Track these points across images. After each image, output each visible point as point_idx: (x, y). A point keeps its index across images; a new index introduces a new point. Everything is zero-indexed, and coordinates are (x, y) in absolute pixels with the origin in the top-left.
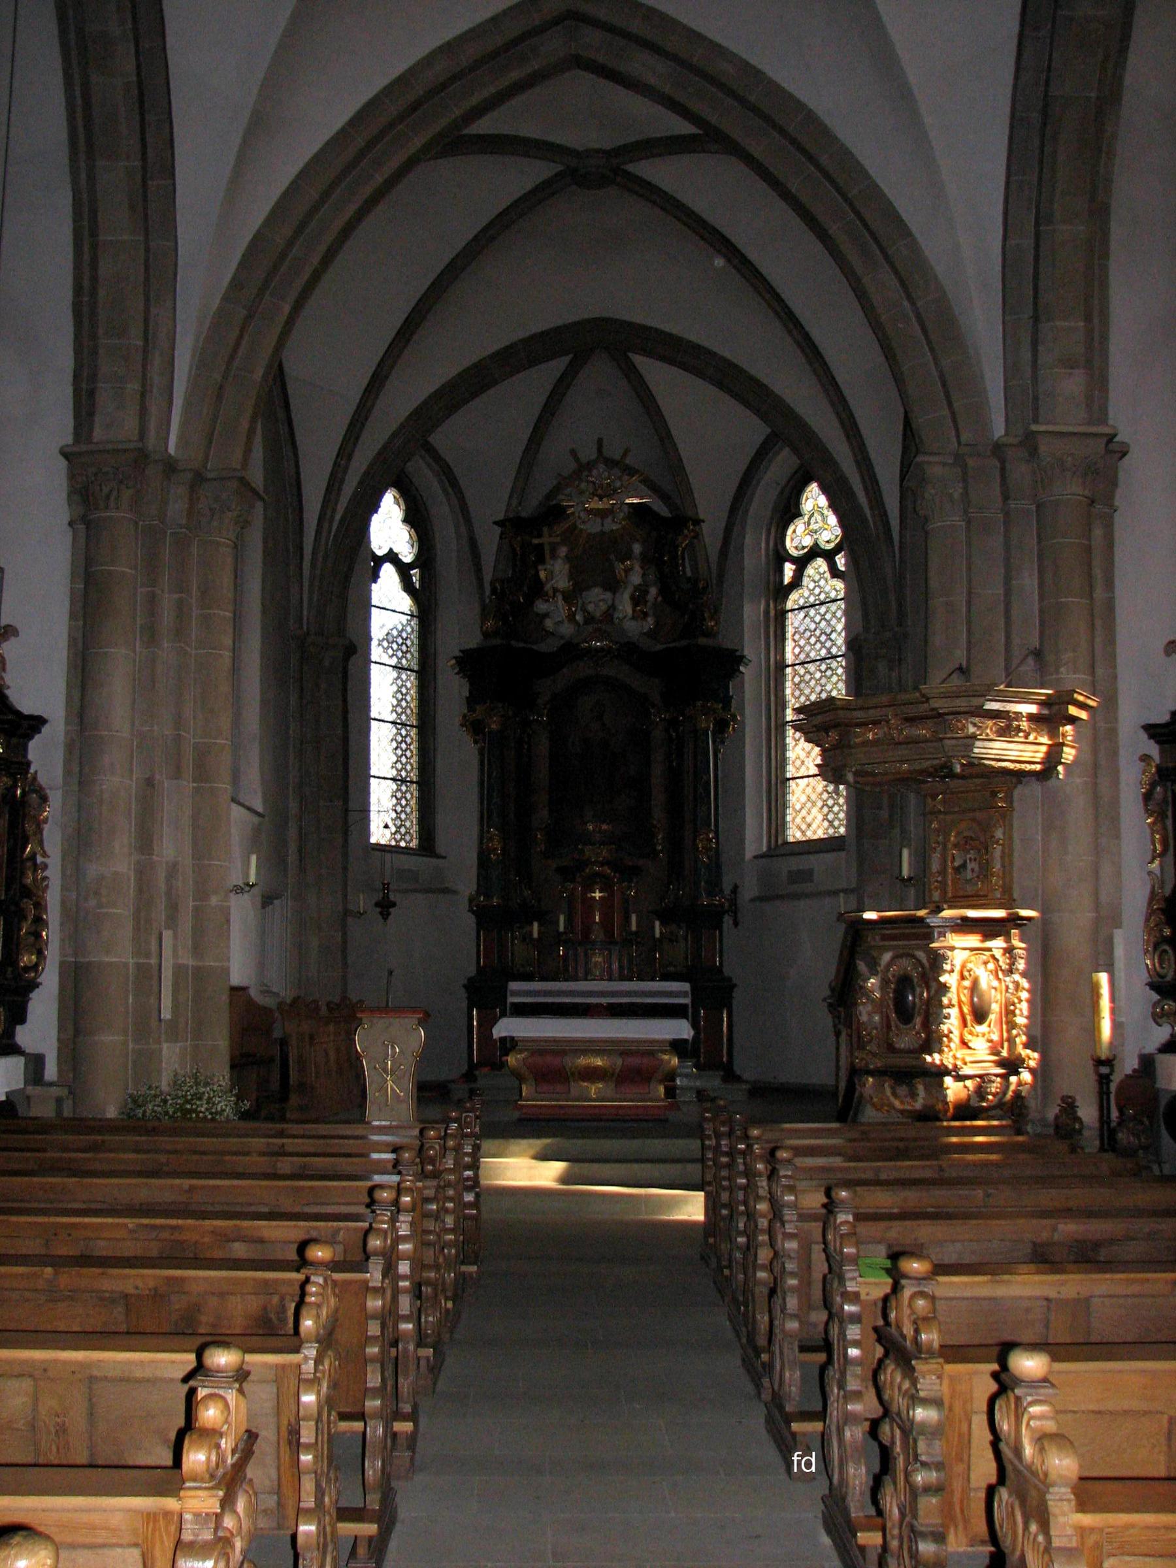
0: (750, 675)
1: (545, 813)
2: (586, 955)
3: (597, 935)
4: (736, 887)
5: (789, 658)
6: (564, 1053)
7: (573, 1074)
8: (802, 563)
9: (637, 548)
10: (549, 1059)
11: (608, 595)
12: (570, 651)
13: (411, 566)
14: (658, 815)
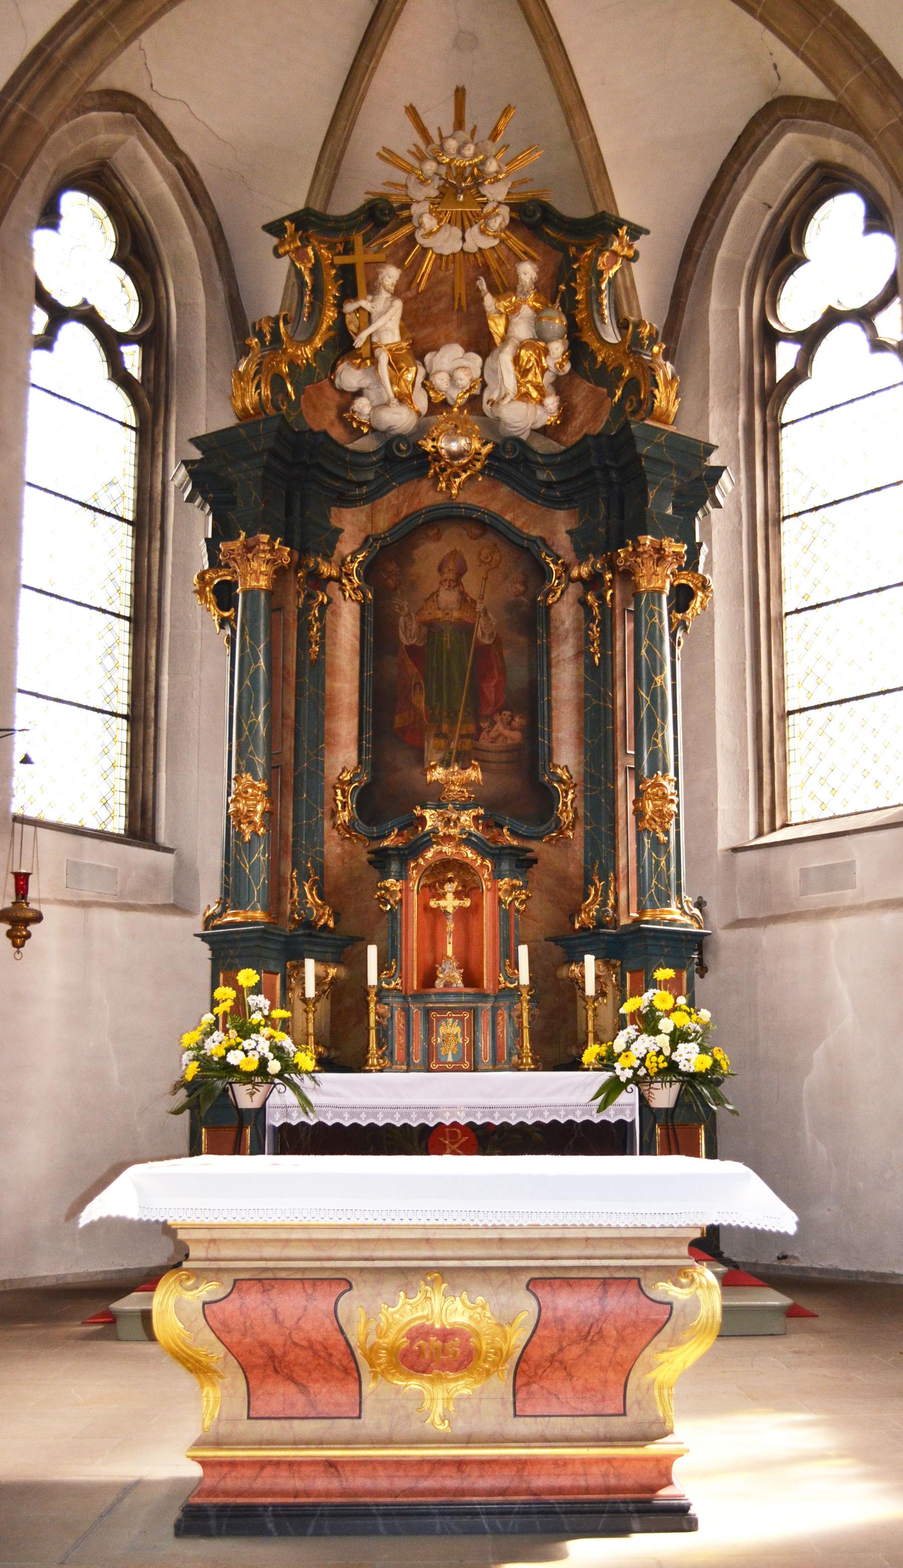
6: (342, 1282)
7: (372, 1353)
8: (810, 339)
9: (527, 272)
10: (290, 1304)
11: (475, 360)
12: (405, 458)
13: (125, 339)
14: (567, 757)
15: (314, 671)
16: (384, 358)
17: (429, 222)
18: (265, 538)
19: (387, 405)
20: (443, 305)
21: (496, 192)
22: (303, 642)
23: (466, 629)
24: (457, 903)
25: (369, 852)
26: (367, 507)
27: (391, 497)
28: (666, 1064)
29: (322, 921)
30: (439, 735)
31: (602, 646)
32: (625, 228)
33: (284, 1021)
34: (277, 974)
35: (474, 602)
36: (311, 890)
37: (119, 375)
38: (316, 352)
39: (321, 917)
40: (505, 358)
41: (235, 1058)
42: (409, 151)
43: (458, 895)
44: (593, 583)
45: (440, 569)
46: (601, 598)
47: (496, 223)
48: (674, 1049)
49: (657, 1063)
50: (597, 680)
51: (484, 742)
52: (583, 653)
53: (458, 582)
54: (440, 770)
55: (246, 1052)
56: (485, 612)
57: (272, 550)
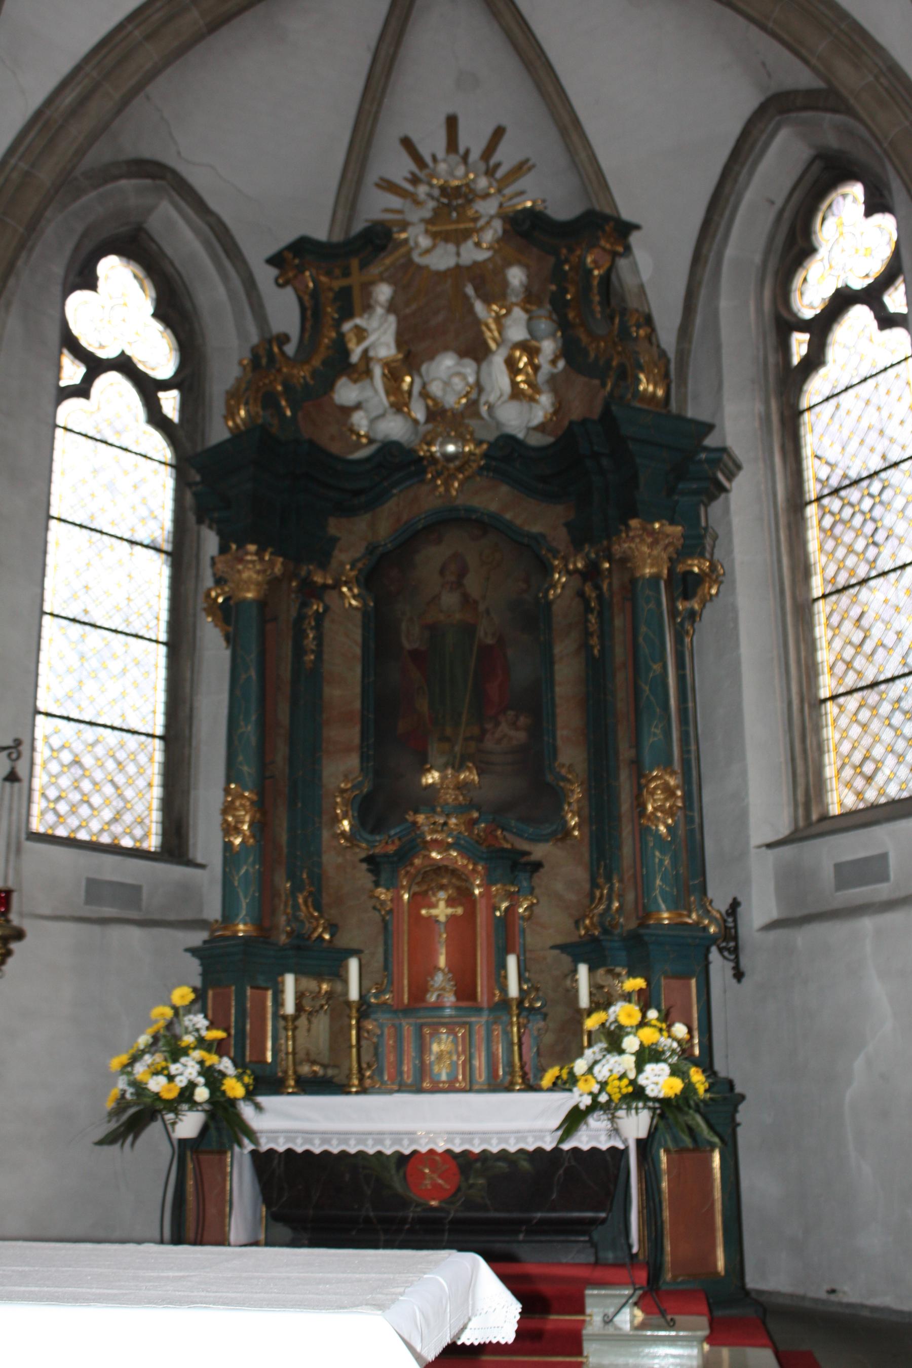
0: (742, 514)
1: (353, 762)
2: (420, 1037)
3: (441, 989)
4: (735, 904)
5: (812, 489)
9: (516, 276)
14: (570, 757)
15: (308, 681)
16: (377, 371)
17: (424, 242)
18: (252, 548)
19: (382, 416)
20: (440, 318)
21: (488, 208)
22: (299, 651)
23: (468, 630)
24: (450, 911)
25: (362, 861)
26: (368, 516)
27: (391, 505)
28: (630, 1089)
29: (316, 935)
30: (444, 739)
31: (602, 637)
32: (612, 224)
33: (220, 1042)
34: (266, 989)
35: (476, 602)
36: (306, 902)
37: (156, 417)
38: (314, 373)
39: (315, 929)
40: (498, 360)
41: (157, 1084)
42: (406, 179)
43: (450, 902)
44: (591, 573)
45: (442, 572)
46: (598, 588)
47: (488, 236)
48: (640, 1069)
49: (620, 1088)
50: (596, 673)
51: (489, 744)
52: (584, 646)
53: (459, 584)
54: (436, 775)
55: (171, 1078)
56: (488, 612)
57: (261, 559)
